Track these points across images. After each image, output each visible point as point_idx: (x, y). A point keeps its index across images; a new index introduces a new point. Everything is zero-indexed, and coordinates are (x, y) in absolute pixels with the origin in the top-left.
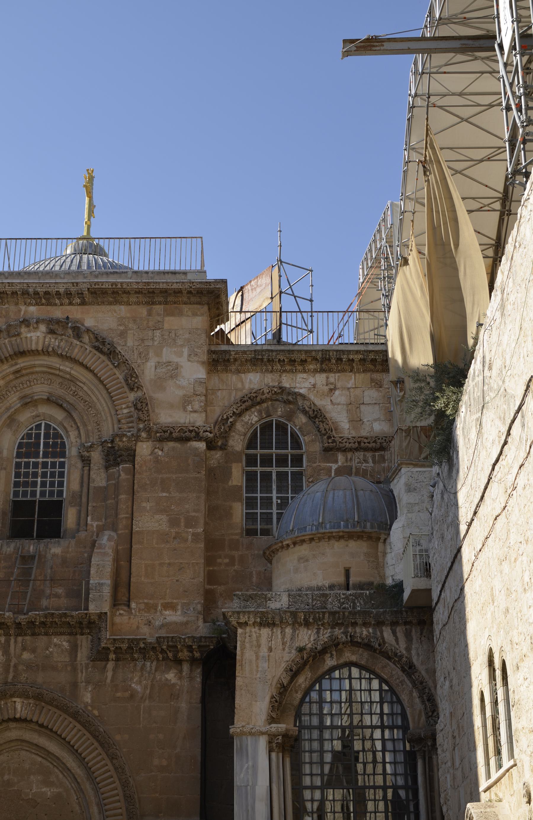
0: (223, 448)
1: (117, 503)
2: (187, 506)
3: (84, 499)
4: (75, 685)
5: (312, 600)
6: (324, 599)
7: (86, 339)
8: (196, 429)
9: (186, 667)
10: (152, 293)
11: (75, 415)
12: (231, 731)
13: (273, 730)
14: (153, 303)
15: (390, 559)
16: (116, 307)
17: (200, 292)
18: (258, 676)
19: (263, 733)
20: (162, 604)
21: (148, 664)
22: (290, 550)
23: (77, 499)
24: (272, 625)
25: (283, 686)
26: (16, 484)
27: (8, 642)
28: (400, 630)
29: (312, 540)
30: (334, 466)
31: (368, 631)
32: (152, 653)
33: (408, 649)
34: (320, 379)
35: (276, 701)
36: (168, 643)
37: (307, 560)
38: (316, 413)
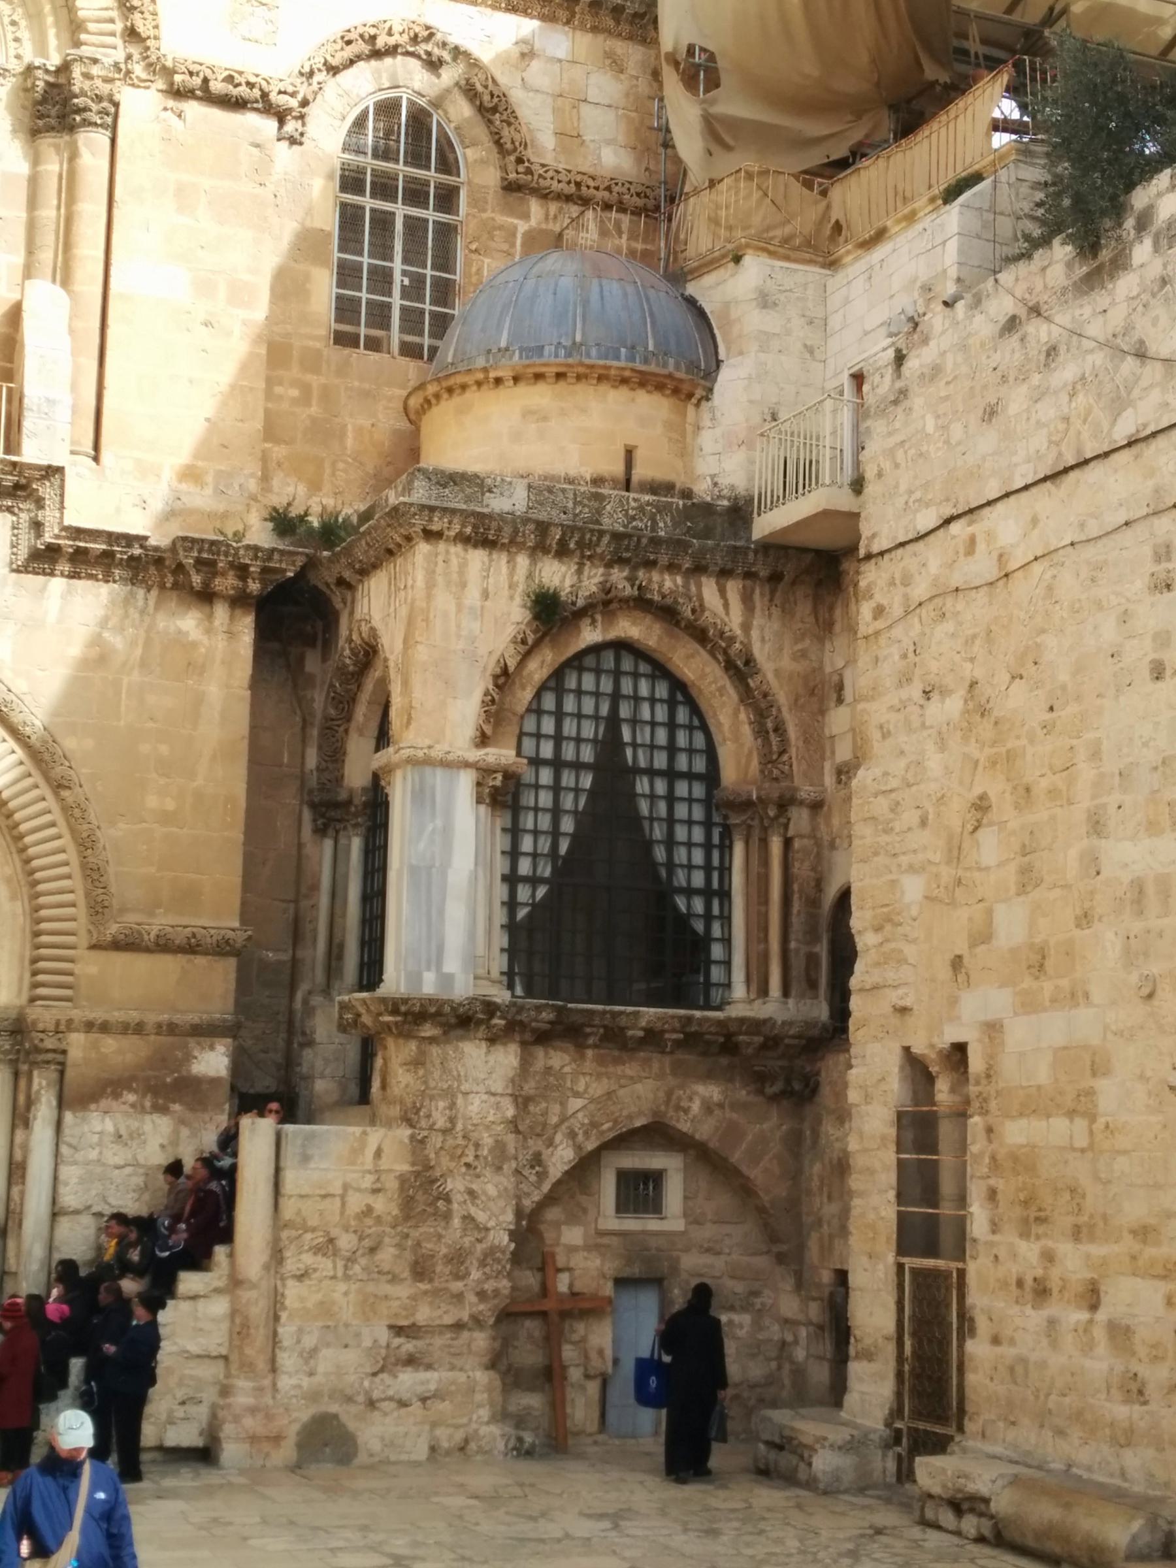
5: (575, 503)
6: (596, 505)
15: (708, 440)
18: (461, 645)
21: (141, 593)
22: (503, 392)
28: (733, 587)
29: (560, 376)
31: (675, 582)
32: (152, 570)
37: (545, 419)
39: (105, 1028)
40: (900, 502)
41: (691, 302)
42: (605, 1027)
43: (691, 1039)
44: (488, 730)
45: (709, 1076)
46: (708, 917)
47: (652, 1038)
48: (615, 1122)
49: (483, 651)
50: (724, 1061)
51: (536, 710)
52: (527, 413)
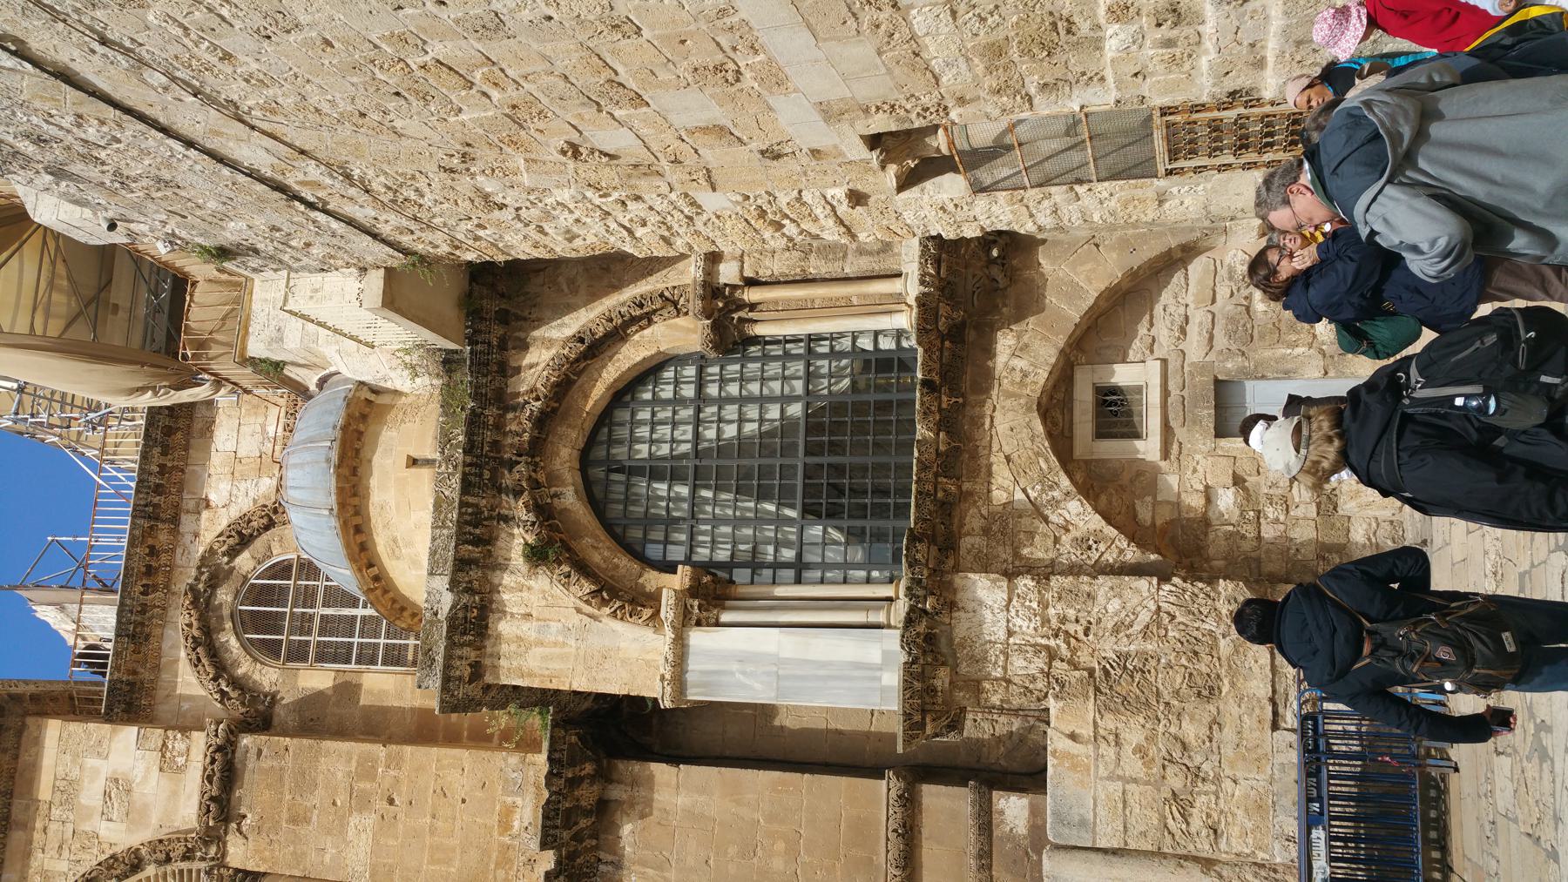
2: (340, 775)
6: (445, 505)
8: (211, 749)
12: (667, 704)
13: (671, 616)
18: (572, 642)
20: (501, 835)
35: (622, 607)
36: (557, 827)
37: (395, 541)
38: (233, 533)
42: (936, 475)
44: (647, 613)
46: (834, 354)
48: (1038, 454)
49: (576, 619)
50: (971, 335)
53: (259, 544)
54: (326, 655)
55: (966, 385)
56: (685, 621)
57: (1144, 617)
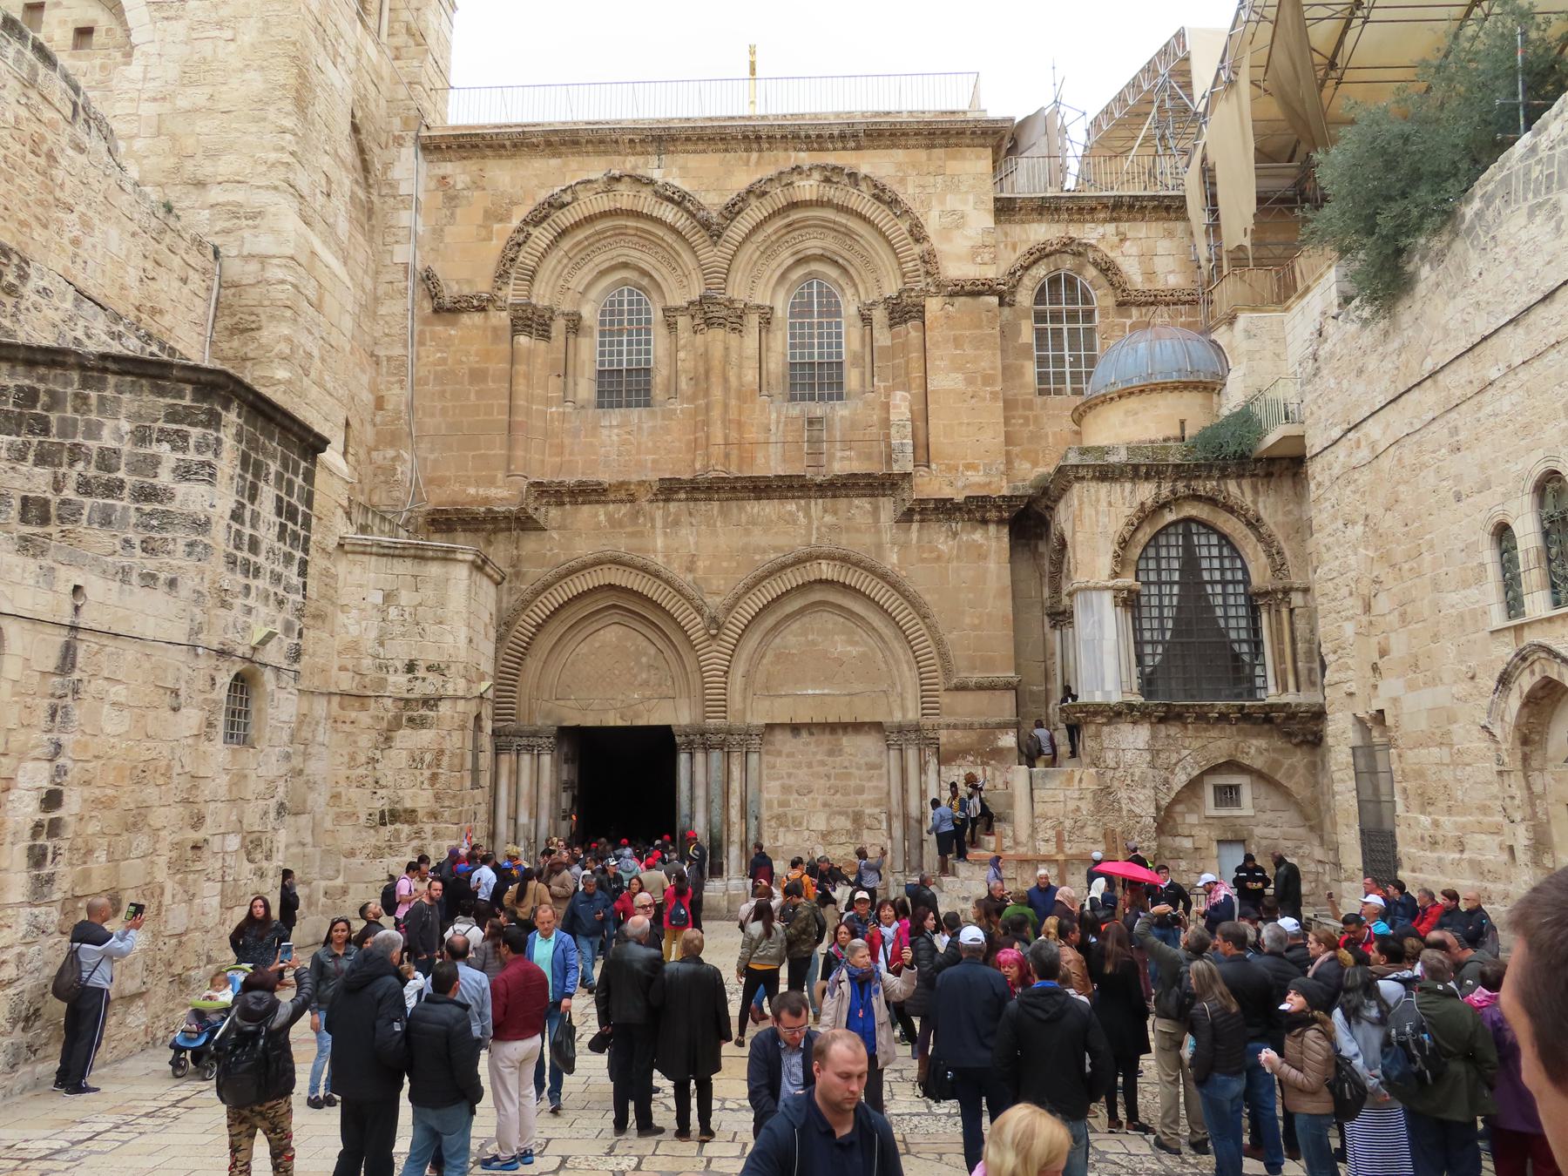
0: (1011, 305)
1: (907, 363)
3: (868, 359)
4: (879, 546)
7: (863, 187)
9: (992, 528)
10: (932, 134)
11: (852, 271)
14: (934, 146)
16: (894, 151)
17: (984, 133)
19: (1108, 588)
23: (857, 360)
24: (1114, 479)
25: (1125, 540)
26: (793, 346)
27: (808, 505)
29: (1142, 391)
30: (1128, 322)
33: (1255, 502)
34: (1110, 228)
39: (955, 727)
40: (1322, 425)
41: (1214, 342)
43: (1246, 716)
45: (1258, 736)
47: (1223, 717)
49: (1111, 531)
51: (1143, 556)
52: (1127, 412)
53: (1102, 281)
54: (1041, 335)
55: (1241, 725)
56: (1118, 590)
57: (1138, 811)
